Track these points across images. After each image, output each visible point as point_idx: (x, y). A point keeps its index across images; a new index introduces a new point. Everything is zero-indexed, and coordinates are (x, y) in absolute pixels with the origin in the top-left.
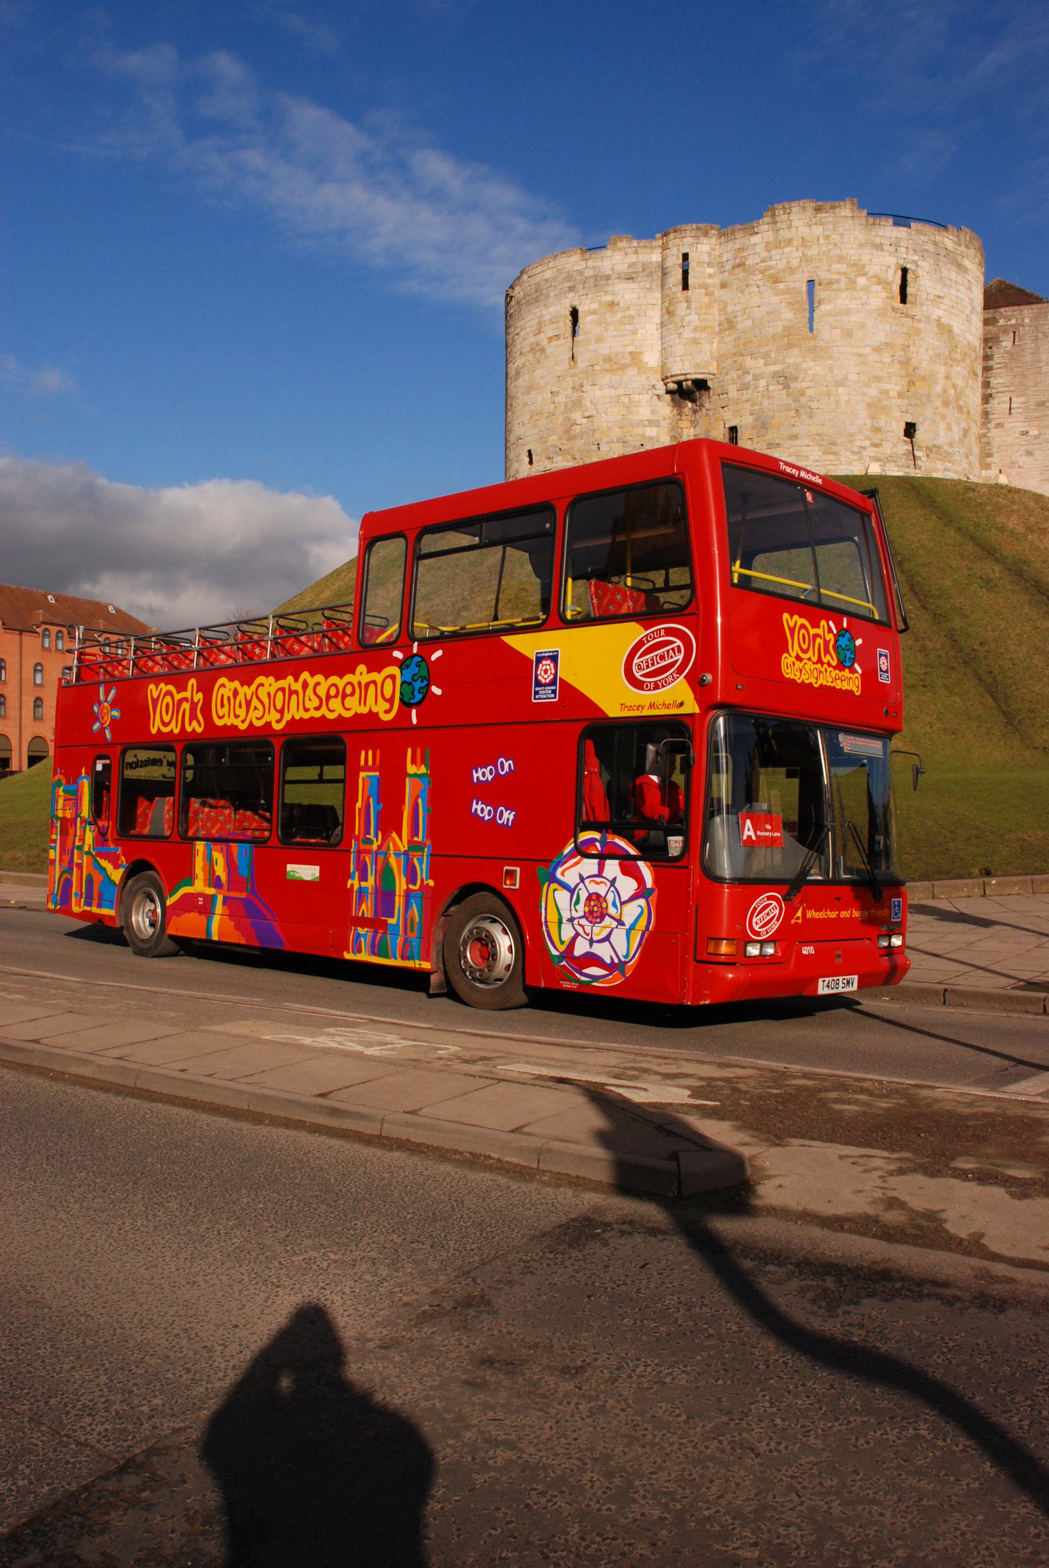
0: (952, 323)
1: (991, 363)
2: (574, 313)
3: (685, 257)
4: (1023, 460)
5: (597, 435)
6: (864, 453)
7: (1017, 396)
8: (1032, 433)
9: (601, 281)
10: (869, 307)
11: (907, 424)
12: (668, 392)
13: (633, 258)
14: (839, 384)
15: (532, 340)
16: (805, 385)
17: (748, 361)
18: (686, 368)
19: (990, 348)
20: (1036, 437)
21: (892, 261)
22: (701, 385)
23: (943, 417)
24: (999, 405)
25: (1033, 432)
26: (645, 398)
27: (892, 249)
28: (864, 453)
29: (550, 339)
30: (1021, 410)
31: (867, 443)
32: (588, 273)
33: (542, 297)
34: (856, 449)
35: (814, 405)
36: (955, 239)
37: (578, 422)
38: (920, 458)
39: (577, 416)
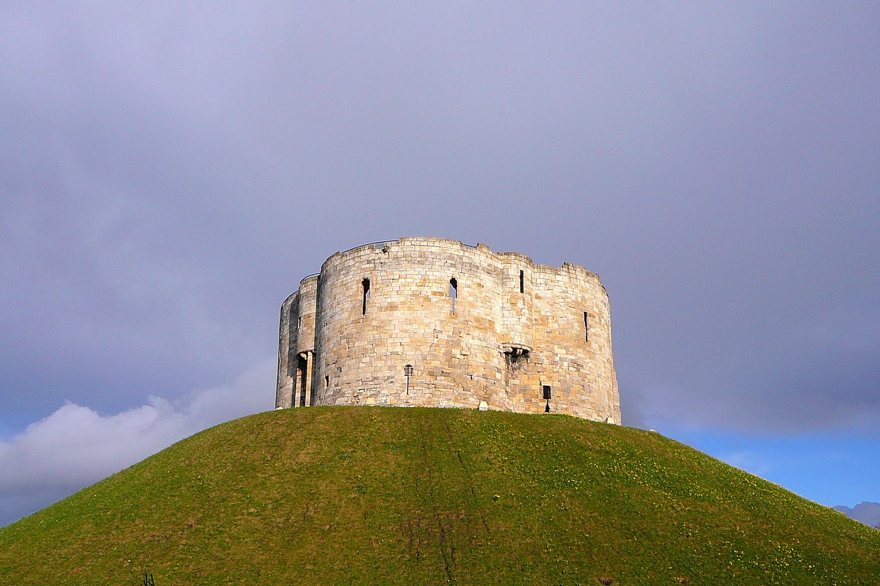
2: (454, 282)
3: (522, 272)
5: (470, 370)
9: (473, 268)
12: (507, 353)
13: (490, 261)
15: (414, 288)
17: (557, 350)
18: (519, 340)
22: (525, 352)
26: (496, 353)
29: (435, 293)
32: (465, 260)
33: (427, 263)
37: (458, 356)
39: (456, 352)
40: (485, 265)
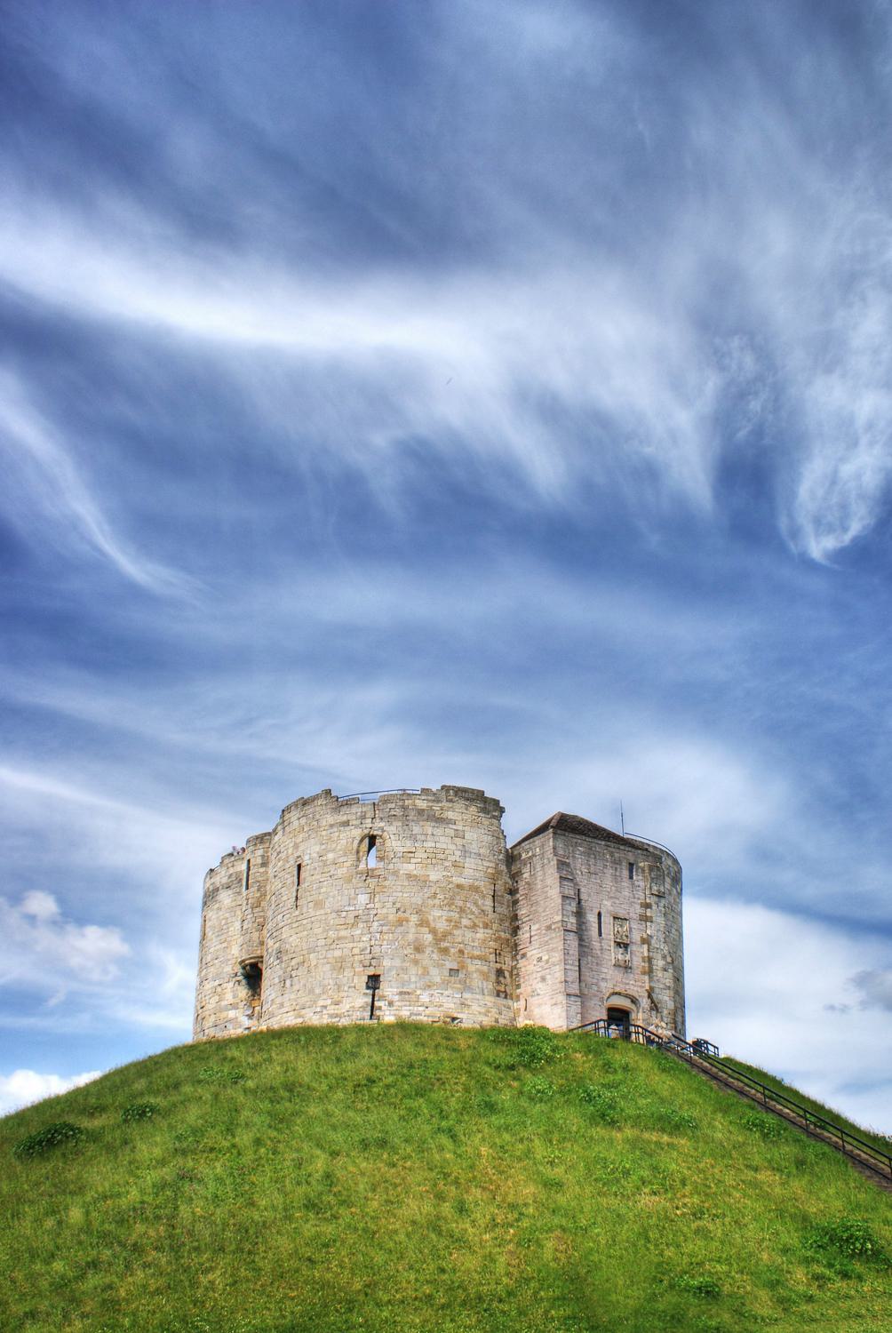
1: (518, 895)
4: (540, 986)
6: (325, 1012)
7: (534, 924)
8: (545, 958)
10: (336, 877)
11: (369, 977)
13: (231, 871)
14: (312, 950)
16: (291, 956)
19: (517, 882)
20: (547, 962)
21: (357, 833)
23: (416, 962)
24: (523, 935)
25: (545, 958)
27: (358, 822)
28: (325, 1012)
30: (536, 937)
31: (329, 1002)
34: (318, 1009)
35: (294, 973)
38: (380, 1008)
40: (225, 880)
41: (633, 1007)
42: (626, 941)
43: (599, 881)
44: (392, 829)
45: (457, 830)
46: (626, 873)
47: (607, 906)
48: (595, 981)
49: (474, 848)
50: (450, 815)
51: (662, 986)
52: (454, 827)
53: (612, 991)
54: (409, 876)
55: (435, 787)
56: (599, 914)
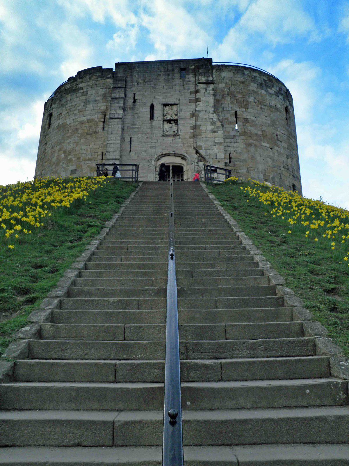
0: (65, 121)
36: (71, 81)
41: (183, 162)
42: (176, 118)
43: (153, 85)
44: (56, 105)
45: (83, 92)
46: (177, 75)
47: (158, 100)
48: (144, 149)
49: (93, 98)
50: (81, 85)
51: (211, 143)
52: (82, 91)
53: (161, 154)
54: (59, 127)
55: (74, 74)
56: (152, 107)
